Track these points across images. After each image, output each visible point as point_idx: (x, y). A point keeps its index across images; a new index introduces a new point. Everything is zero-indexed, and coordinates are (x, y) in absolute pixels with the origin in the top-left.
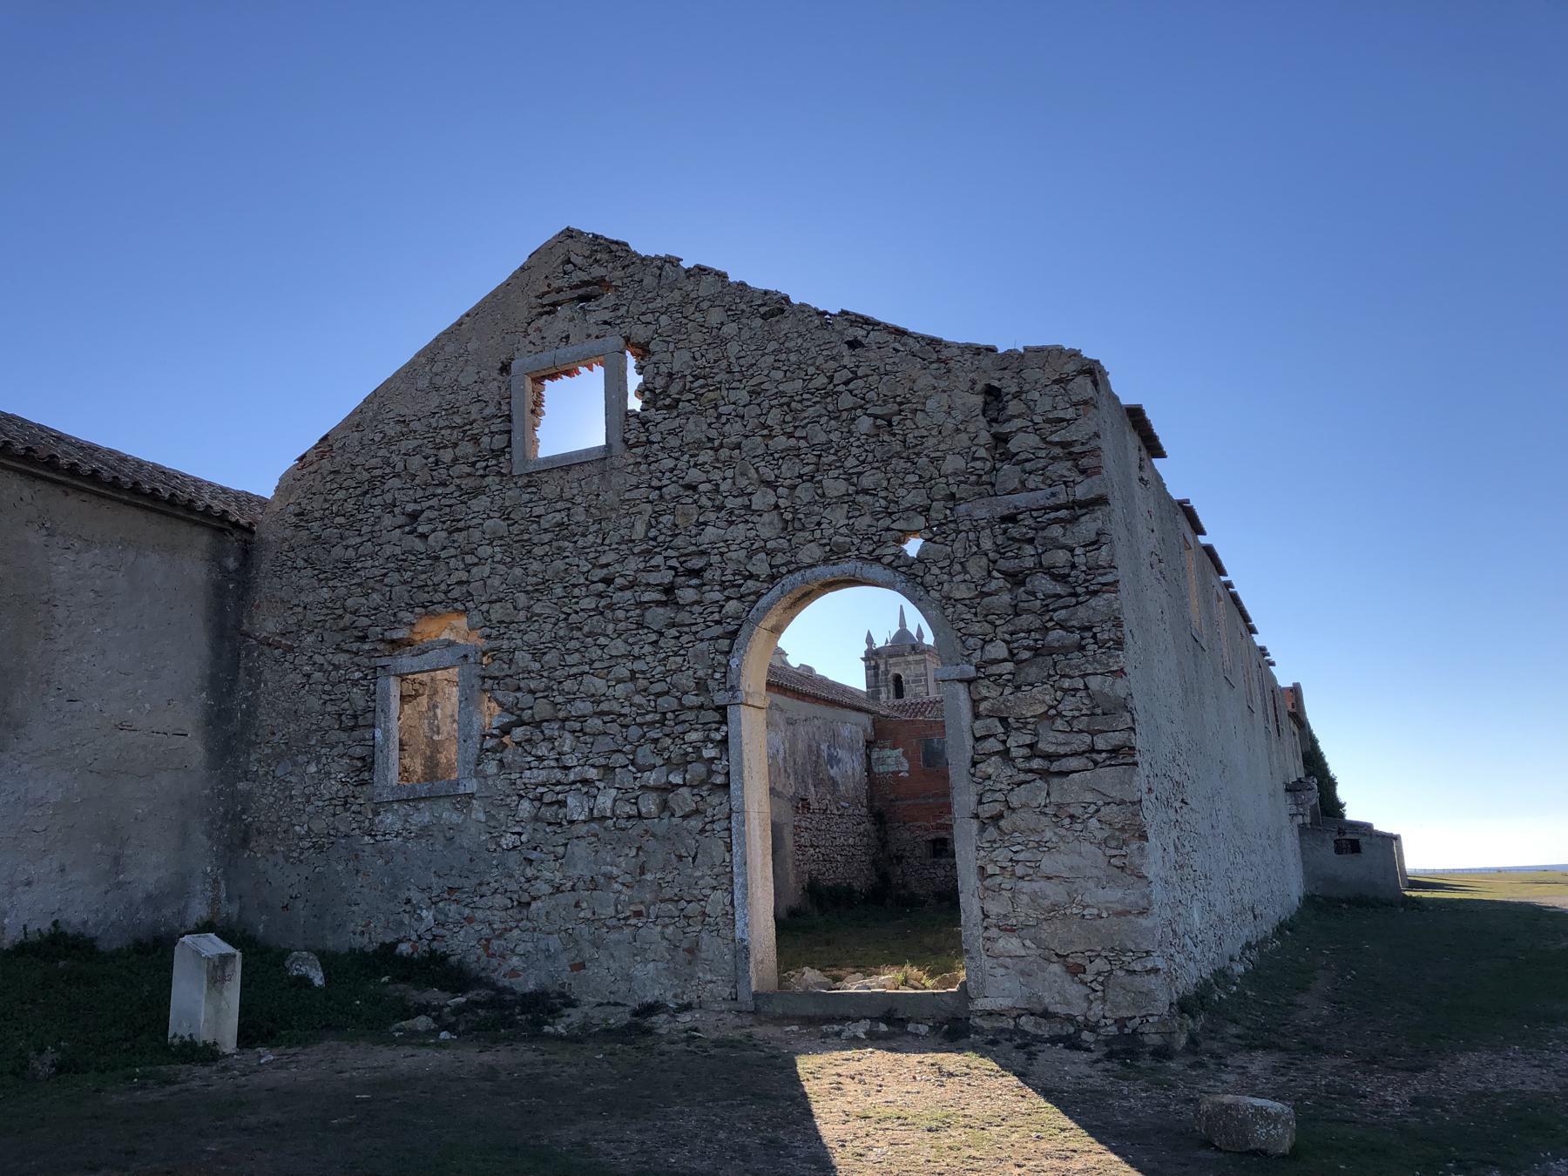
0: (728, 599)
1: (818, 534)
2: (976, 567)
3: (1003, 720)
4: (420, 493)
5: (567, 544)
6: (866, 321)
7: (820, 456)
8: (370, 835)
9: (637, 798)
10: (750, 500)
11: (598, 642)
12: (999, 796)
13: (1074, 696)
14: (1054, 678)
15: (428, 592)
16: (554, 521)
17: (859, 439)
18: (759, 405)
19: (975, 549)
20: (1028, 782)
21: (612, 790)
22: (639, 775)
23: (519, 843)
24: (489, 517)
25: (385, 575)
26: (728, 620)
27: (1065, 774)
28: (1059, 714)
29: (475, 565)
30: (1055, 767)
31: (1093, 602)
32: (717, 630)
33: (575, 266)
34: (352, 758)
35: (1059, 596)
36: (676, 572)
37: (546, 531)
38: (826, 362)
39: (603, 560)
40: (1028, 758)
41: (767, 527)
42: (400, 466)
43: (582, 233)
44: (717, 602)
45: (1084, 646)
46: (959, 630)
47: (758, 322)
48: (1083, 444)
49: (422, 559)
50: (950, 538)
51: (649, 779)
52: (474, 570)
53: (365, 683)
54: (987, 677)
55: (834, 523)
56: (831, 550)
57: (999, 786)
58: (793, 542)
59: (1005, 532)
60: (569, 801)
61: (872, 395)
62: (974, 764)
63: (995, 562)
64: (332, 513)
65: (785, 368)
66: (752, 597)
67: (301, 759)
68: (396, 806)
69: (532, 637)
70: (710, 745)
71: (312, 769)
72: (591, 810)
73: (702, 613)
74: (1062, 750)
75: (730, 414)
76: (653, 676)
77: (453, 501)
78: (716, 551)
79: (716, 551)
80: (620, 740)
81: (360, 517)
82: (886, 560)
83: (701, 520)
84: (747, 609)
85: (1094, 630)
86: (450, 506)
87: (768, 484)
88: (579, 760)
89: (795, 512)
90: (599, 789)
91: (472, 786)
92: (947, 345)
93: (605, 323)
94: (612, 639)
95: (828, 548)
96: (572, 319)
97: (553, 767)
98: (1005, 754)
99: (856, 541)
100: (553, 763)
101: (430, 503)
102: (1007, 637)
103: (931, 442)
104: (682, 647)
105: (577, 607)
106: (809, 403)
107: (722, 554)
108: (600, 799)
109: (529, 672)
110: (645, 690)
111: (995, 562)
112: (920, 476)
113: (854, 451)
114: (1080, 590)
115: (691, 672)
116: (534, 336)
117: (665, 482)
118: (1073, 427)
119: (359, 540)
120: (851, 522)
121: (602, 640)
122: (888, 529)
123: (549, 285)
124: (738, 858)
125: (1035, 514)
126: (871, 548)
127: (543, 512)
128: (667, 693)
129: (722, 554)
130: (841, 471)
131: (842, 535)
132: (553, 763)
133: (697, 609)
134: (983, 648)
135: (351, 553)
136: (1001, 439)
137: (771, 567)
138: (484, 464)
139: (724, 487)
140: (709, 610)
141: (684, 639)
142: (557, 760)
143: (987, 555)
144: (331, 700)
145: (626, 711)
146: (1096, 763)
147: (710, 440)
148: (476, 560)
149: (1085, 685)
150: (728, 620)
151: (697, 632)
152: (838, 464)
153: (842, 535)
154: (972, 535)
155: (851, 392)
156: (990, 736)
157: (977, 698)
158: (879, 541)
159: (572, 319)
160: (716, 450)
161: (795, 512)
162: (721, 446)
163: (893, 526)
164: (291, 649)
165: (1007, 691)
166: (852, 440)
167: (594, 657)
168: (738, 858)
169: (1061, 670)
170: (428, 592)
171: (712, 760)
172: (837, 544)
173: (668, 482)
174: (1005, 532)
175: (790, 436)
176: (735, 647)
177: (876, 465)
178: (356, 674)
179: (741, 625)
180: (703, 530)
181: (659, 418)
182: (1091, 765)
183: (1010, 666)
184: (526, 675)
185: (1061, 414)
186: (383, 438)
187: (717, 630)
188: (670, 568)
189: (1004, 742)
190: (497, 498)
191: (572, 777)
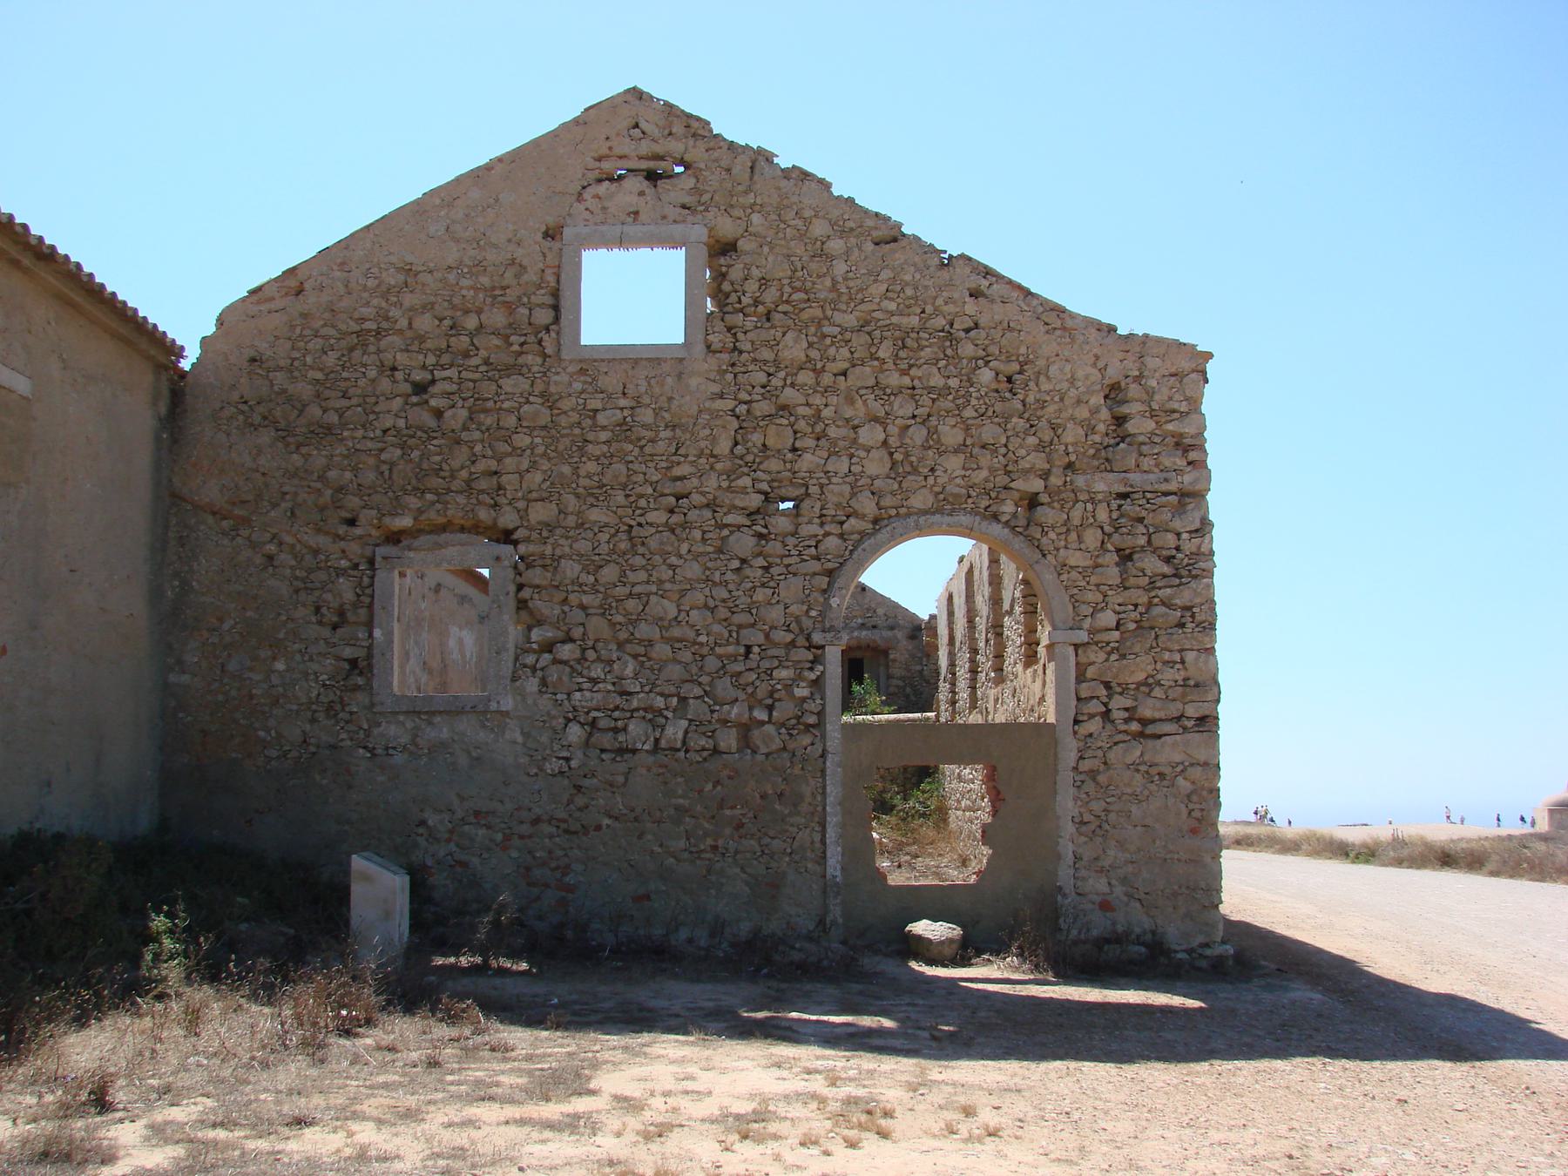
1: (931, 480)
2: (1092, 538)
3: (1107, 685)
4: (431, 360)
5: (631, 447)
6: (988, 272)
8: (365, 748)
9: (713, 732)
11: (668, 561)
12: (1100, 753)
13: (1172, 668)
14: (1156, 650)
15: (444, 478)
16: (614, 418)
18: (869, 334)
20: (1125, 741)
21: (683, 721)
22: (717, 708)
23: (567, 769)
24: (528, 402)
25: (382, 450)
27: (1160, 737)
28: (1159, 684)
29: (510, 455)
30: (1150, 730)
31: (1193, 584)
32: (815, 566)
33: (643, 133)
34: (338, 658)
35: (1165, 576)
37: (604, 428)
38: (946, 303)
39: (677, 471)
40: (1126, 721)
41: (876, 465)
42: (403, 323)
43: (652, 97)
44: (816, 536)
45: (1184, 624)
47: (869, 247)
48: (1192, 437)
49: (436, 438)
51: (729, 712)
52: (508, 461)
53: (355, 573)
54: (1096, 643)
55: (949, 472)
57: (1100, 744)
58: (904, 485)
59: (1120, 506)
60: (631, 727)
61: (994, 349)
62: (1076, 722)
63: (1110, 535)
64: (305, 365)
65: (899, 300)
67: (265, 653)
68: (401, 718)
69: (583, 546)
71: (280, 666)
72: (657, 741)
73: (797, 546)
74: (1157, 715)
75: (835, 337)
76: (737, 606)
77: (477, 376)
78: (814, 481)
79: (814, 481)
80: (694, 670)
81: (345, 375)
82: (1004, 518)
84: (850, 548)
85: (1194, 610)
86: (474, 381)
87: (876, 419)
88: (642, 687)
89: (907, 455)
90: (667, 718)
91: (508, 703)
92: (1073, 316)
93: (684, 207)
94: (686, 560)
96: (641, 194)
97: (609, 691)
98: (1106, 715)
100: (610, 687)
101: (447, 373)
102: (1117, 608)
103: (1051, 409)
105: (642, 520)
106: (927, 343)
108: (670, 731)
109: (581, 585)
110: (725, 620)
111: (1110, 535)
113: (974, 402)
114: (1184, 572)
116: (590, 202)
117: (756, 397)
118: (1187, 420)
119: (345, 403)
120: (967, 473)
121: (673, 560)
123: (610, 148)
124: (832, 799)
125: (1149, 495)
126: (988, 504)
127: (599, 406)
128: (753, 625)
132: (610, 687)
133: (791, 541)
135: (334, 418)
136: (1120, 420)
138: (522, 339)
139: (826, 413)
140: (807, 543)
142: (614, 684)
143: (1102, 528)
144: (306, 588)
145: (703, 639)
146: (1185, 728)
149: (1182, 658)
151: (790, 565)
153: (958, 486)
155: (972, 341)
156: (1093, 698)
158: (997, 498)
159: (641, 194)
161: (907, 455)
163: (1012, 485)
164: (246, 521)
165: (1114, 657)
166: (971, 389)
167: (665, 577)
168: (832, 799)
169: (1164, 642)
170: (444, 478)
171: (804, 700)
174: (1120, 506)
175: (904, 373)
178: (342, 562)
180: (800, 456)
181: (749, 325)
182: (1181, 731)
183: (1116, 635)
184: (576, 588)
185: (1176, 406)
186: (378, 286)
187: (815, 566)
188: (760, 492)
189: (1105, 705)
190: (539, 381)
191: (635, 704)
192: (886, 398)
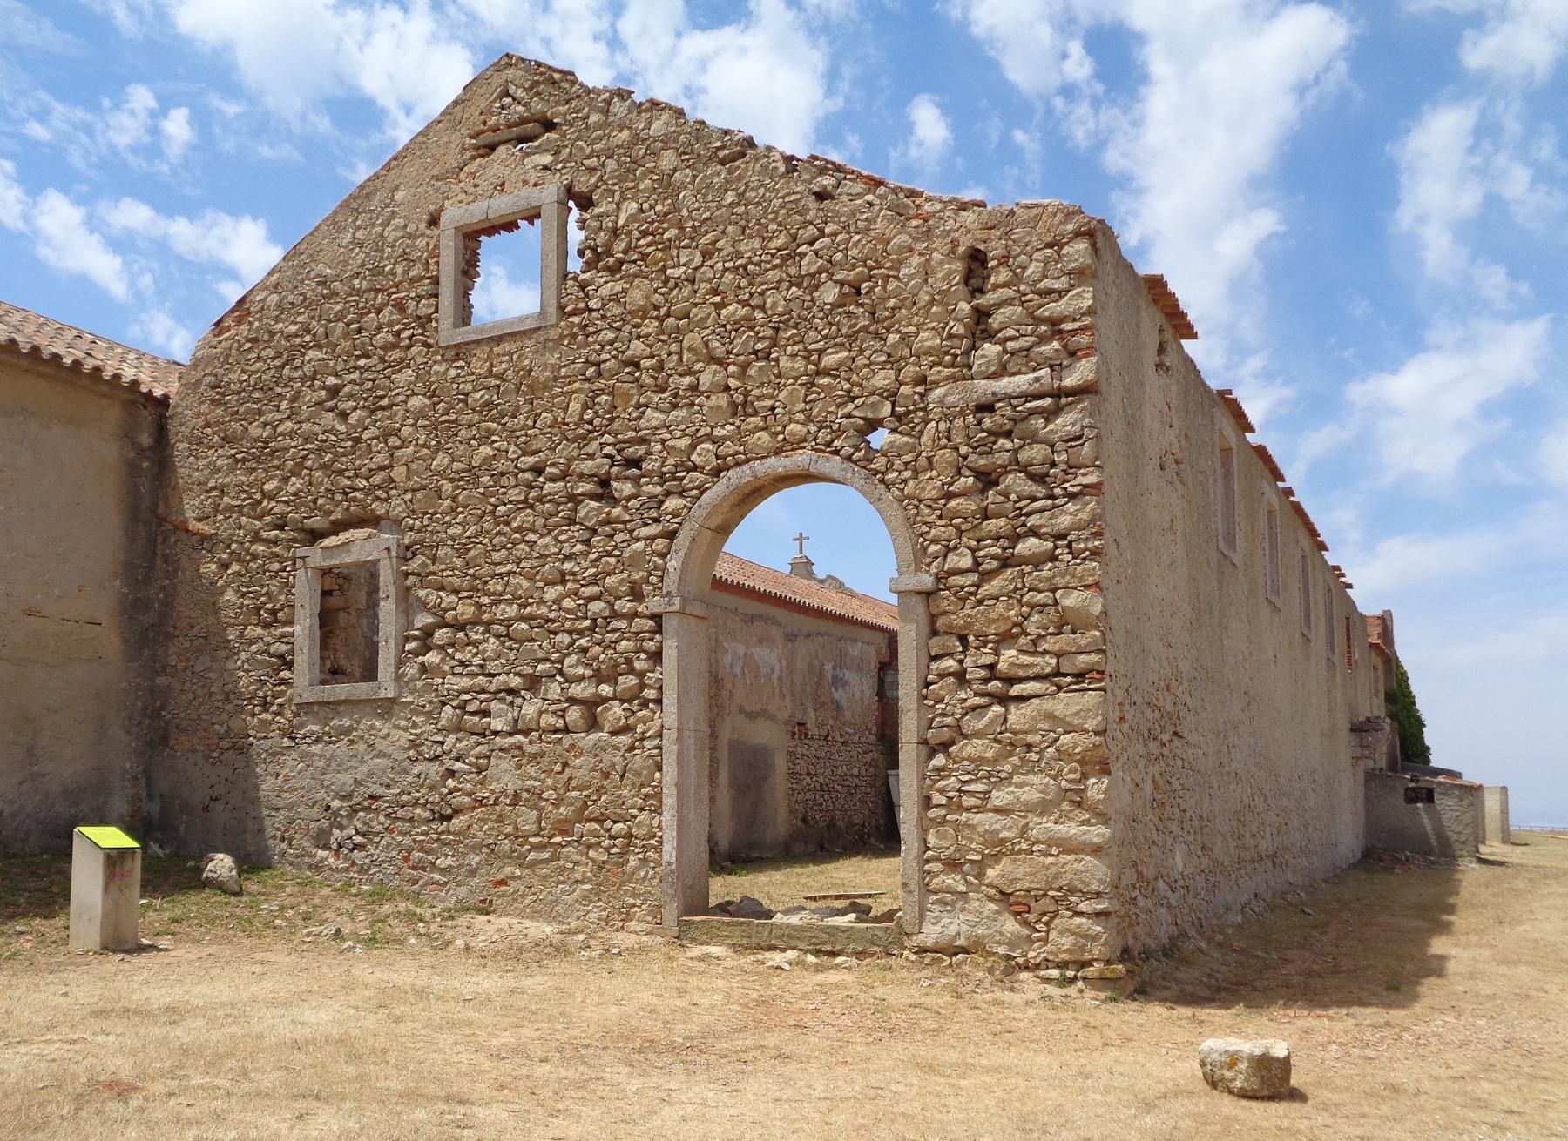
0: (668, 494)
3: (963, 639)
7: (777, 330)
10: (698, 379)
17: (822, 310)
18: (712, 267)
19: (944, 441)
24: (414, 394)
26: (668, 517)
27: (1022, 699)
29: (399, 448)
30: (1016, 690)
33: (514, 99)
36: (613, 461)
40: (986, 681)
46: (921, 535)
48: (1074, 320)
50: (918, 429)
56: (784, 439)
66: (695, 492)
70: (643, 656)
74: (1022, 673)
83: (642, 400)
93: (545, 168)
95: (781, 437)
98: (961, 677)
99: (813, 429)
101: (352, 376)
104: (616, 547)
106: (769, 266)
107: (663, 441)
111: (965, 458)
112: (889, 356)
114: (1058, 491)
115: (625, 575)
117: (604, 356)
121: (531, 537)
122: (849, 416)
126: (828, 438)
129: (663, 441)
130: (801, 347)
131: (797, 422)
134: (945, 556)
137: (718, 458)
139: (671, 363)
141: (619, 538)
147: (656, 308)
148: (398, 443)
150: (668, 517)
152: (797, 339)
154: (942, 426)
157: (935, 611)
158: (839, 430)
160: (661, 320)
162: (668, 315)
163: (855, 413)
172: (791, 434)
173: (608, 356)
176: (673, 548)
177: (838, 340)
179: (680, 524)
192: (727, 335)
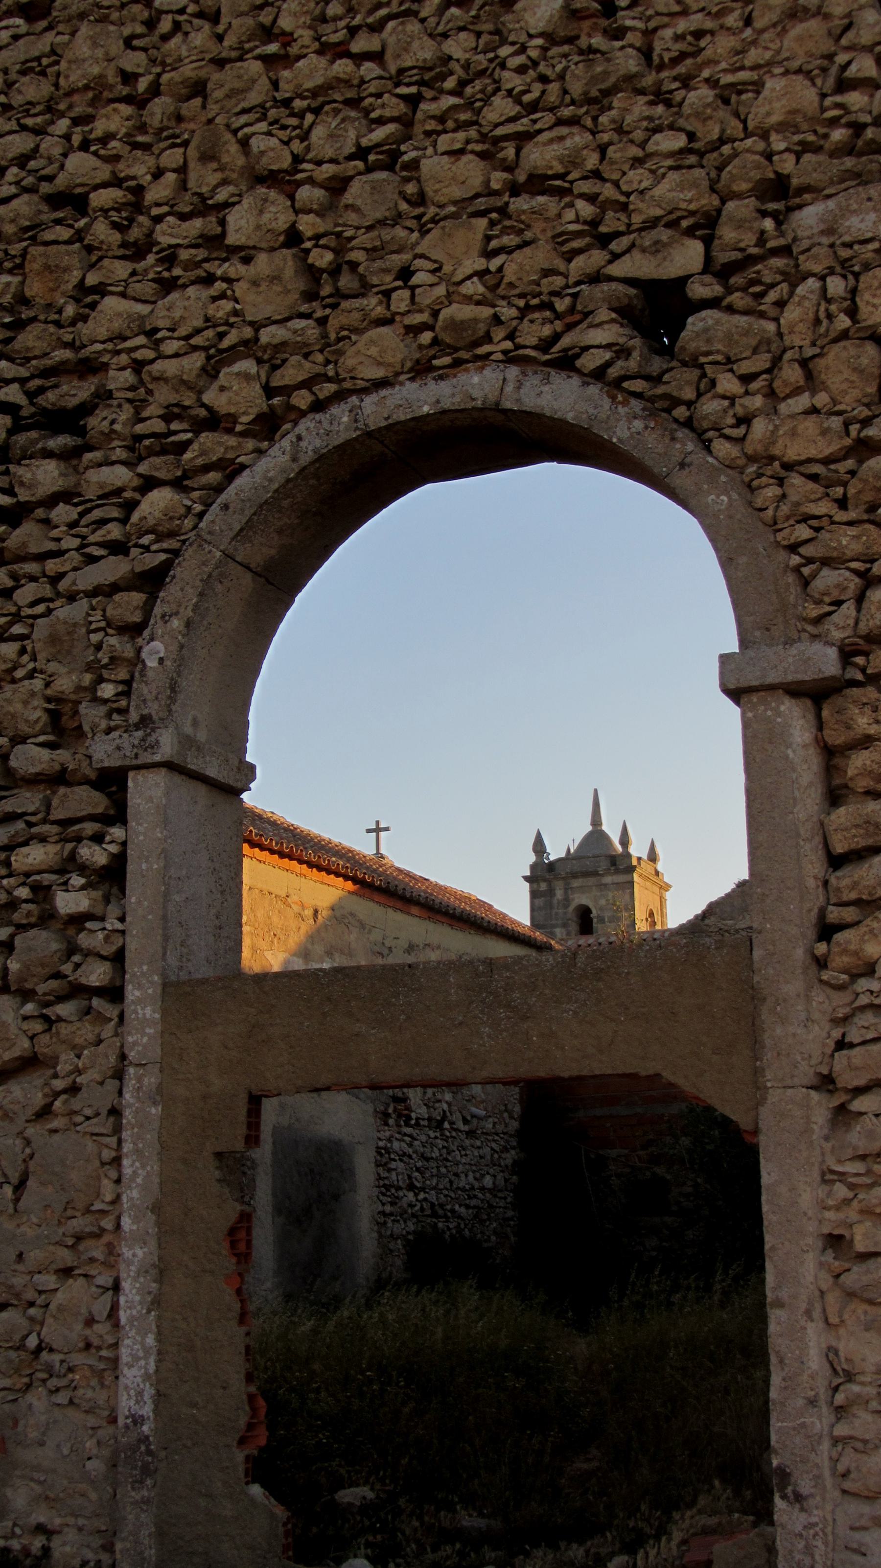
0: (149, 484)
1: (400, 300)
7: (413, 101)
10: (222, 223)
17: (523, 49)
19: (843, 322)
26: (146, 540)
36: (17, 418)
44: (118, 492)
46: (793, 548)
50: (773, 296)
55: (447, 269)
56: (435, 341)
58: (333, 324)
66: (213, 477)
70: (77, 881)
75: (182, 11)
79: (124, 359)
82: (590, 361)
83: (92, 279)
84: (198, 508)
95: (426, 337)
99: (507, 312)
104: (17, 617)
107: (138, 366)
112: (691, 136)
115: (37, 683)
122: (596, 278)
126: (547, 331)
129: (138, 366)
130: (473, 133)
131: (468, 299)
134: (860, 599)
137: (269, 391)
139: (157, 192)
140: (97, 514)
141: (26, 594)
147: (128, 78)
150: (146, 540)
152: (463, 117)
153: (468, 299)
154: (836, 286)
157: (835, 737)
158: (572, 310)
160: (140, 102)
162: (155, 90)
166: (504, 51)
168: (135, 1194)
171: (78, 920)
172: (454, 325)
173: (13, 190)
175: (339, 51)
176: (158, 610)
177: (567, 112)
179: (176, 553)
180: (93, 306)
192: (294, 121)
